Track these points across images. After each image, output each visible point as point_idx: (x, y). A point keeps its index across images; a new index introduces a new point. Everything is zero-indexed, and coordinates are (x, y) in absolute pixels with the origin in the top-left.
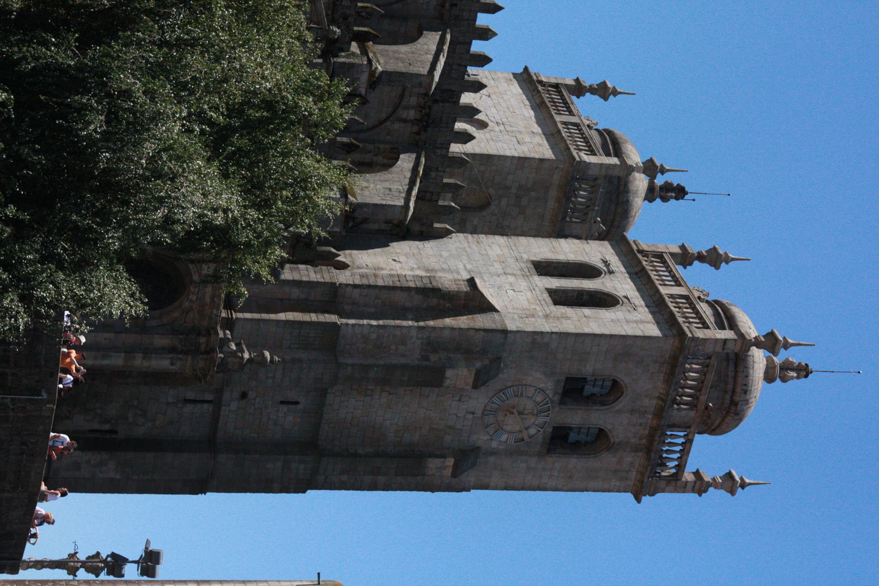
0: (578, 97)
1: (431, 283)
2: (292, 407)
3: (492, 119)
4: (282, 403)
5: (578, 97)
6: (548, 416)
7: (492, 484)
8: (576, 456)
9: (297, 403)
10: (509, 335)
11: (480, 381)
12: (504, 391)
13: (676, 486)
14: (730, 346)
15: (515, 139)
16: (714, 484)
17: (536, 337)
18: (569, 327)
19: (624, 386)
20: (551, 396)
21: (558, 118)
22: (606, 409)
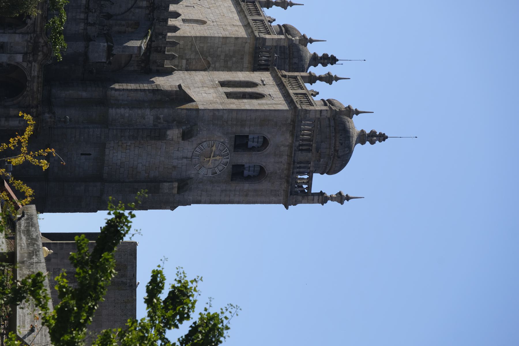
0: (268, 8)
1: (157, 87)
2: (88, 156)
3: (210, 20)
4: (82, 154)
5: (268, 8)
6: (228, 159)
7: (203, 201)
8: (248, 182)
9: (90, 154)
10: (200, 111)
11: (186, 136)
12: (201, 144)
13: (308, 199)
14: (324, 113)
15: (222, 29)
16: (332, 198)
17: (215, 112)
18: (233, 107)
19: (268, 139)
20: (228, 146)
21: (250, 18)
22: (260, 153)
